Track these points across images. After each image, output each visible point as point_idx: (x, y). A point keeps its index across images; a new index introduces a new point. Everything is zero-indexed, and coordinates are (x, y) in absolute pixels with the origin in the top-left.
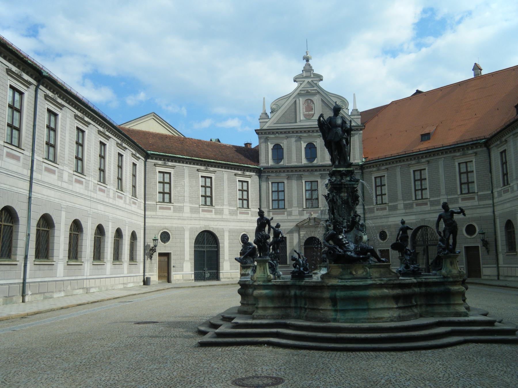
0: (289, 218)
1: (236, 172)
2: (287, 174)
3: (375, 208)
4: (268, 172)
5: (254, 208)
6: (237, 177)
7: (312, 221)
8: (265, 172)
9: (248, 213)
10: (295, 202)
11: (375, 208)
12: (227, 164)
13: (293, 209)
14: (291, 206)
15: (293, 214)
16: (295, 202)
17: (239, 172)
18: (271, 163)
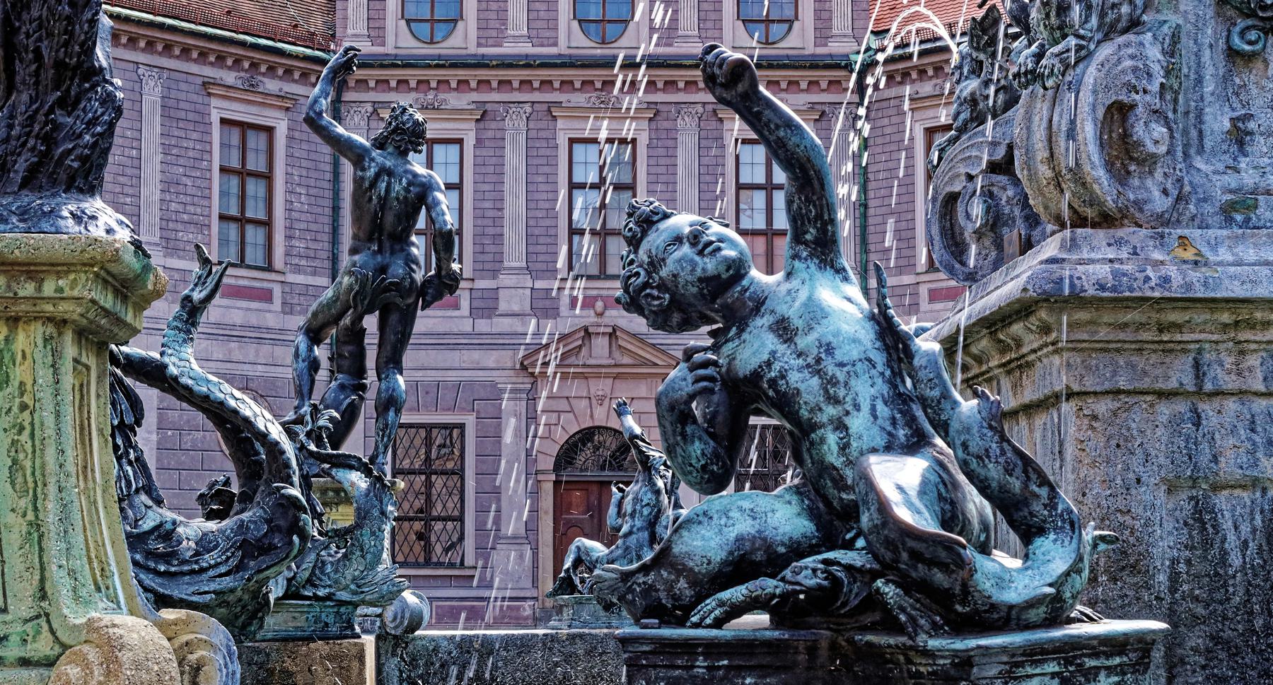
0: (483, 325)
1: (208, 71)
2: (475, 96)
3: (923, 291)
4: (383, 83)
5: (298, 269)
6: (214, 102)
7: (600, 345)
8: (362, 83)
9: (266, 296)
10: (515, 251)
11: (923, 291)
12: (161, 26)
13: (505, 280)
14: (492, 265)
15: (503, 306)
16: (515, 251)
17: (230, 77)
18: (399, 40)
